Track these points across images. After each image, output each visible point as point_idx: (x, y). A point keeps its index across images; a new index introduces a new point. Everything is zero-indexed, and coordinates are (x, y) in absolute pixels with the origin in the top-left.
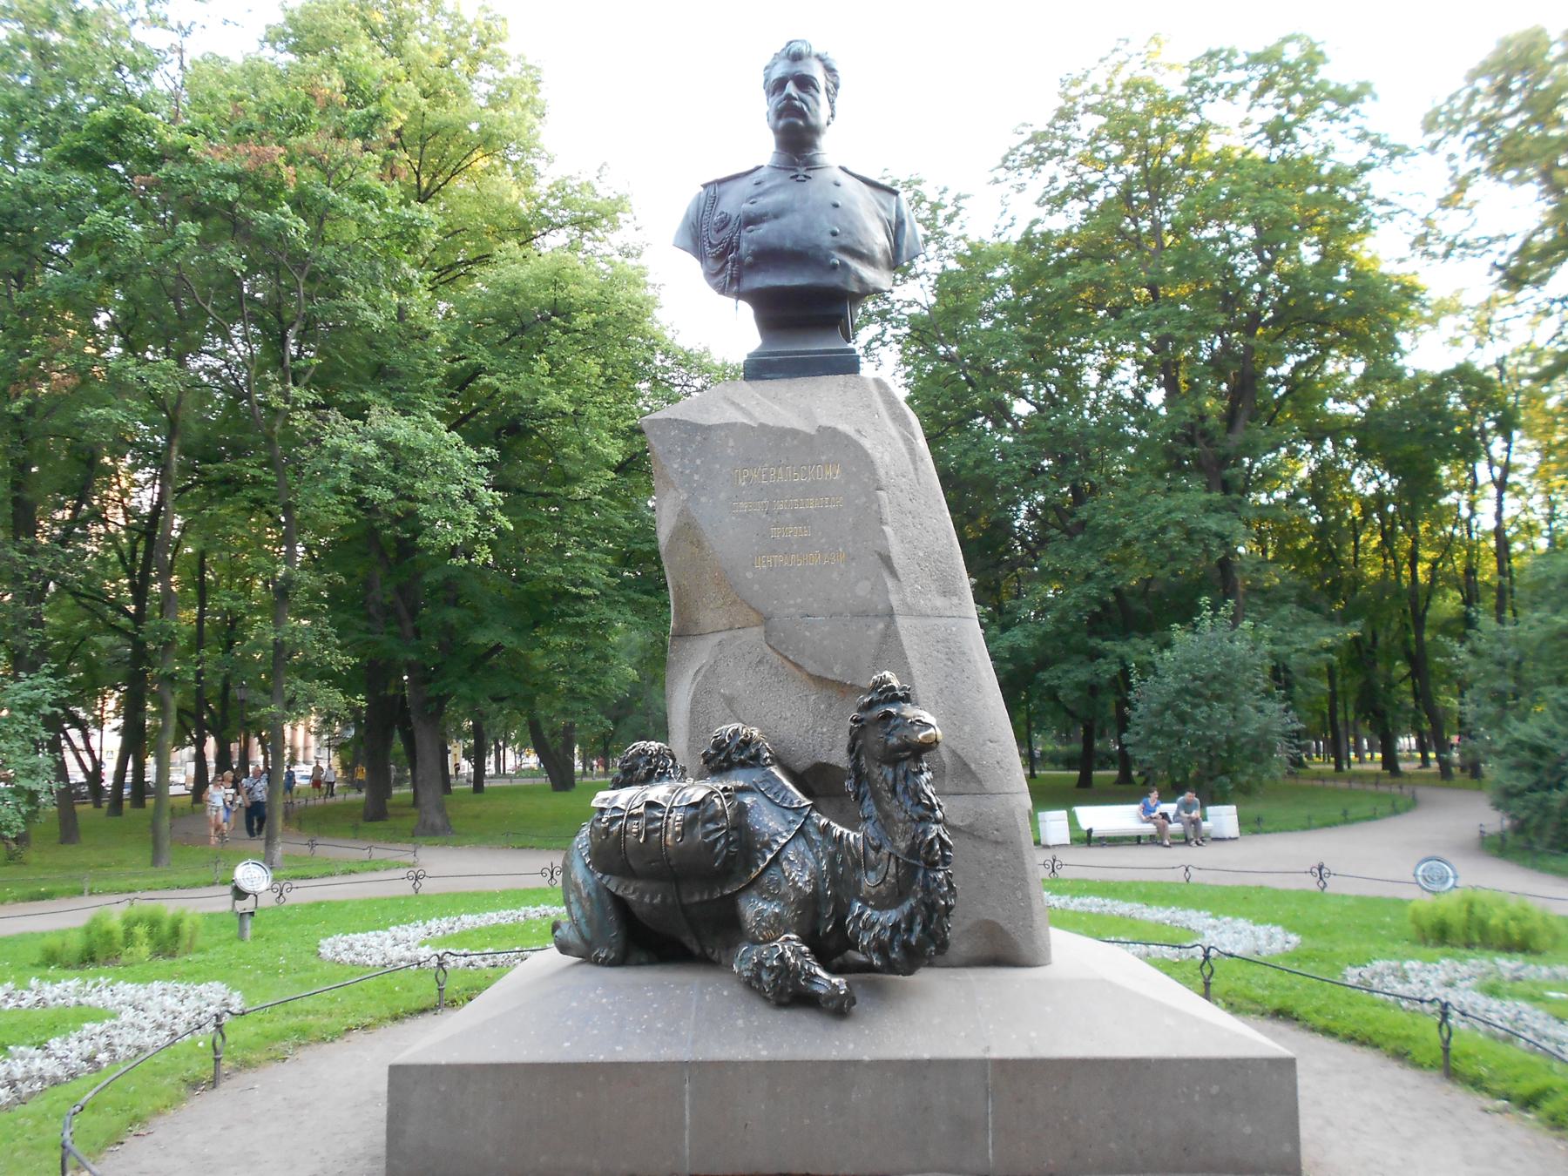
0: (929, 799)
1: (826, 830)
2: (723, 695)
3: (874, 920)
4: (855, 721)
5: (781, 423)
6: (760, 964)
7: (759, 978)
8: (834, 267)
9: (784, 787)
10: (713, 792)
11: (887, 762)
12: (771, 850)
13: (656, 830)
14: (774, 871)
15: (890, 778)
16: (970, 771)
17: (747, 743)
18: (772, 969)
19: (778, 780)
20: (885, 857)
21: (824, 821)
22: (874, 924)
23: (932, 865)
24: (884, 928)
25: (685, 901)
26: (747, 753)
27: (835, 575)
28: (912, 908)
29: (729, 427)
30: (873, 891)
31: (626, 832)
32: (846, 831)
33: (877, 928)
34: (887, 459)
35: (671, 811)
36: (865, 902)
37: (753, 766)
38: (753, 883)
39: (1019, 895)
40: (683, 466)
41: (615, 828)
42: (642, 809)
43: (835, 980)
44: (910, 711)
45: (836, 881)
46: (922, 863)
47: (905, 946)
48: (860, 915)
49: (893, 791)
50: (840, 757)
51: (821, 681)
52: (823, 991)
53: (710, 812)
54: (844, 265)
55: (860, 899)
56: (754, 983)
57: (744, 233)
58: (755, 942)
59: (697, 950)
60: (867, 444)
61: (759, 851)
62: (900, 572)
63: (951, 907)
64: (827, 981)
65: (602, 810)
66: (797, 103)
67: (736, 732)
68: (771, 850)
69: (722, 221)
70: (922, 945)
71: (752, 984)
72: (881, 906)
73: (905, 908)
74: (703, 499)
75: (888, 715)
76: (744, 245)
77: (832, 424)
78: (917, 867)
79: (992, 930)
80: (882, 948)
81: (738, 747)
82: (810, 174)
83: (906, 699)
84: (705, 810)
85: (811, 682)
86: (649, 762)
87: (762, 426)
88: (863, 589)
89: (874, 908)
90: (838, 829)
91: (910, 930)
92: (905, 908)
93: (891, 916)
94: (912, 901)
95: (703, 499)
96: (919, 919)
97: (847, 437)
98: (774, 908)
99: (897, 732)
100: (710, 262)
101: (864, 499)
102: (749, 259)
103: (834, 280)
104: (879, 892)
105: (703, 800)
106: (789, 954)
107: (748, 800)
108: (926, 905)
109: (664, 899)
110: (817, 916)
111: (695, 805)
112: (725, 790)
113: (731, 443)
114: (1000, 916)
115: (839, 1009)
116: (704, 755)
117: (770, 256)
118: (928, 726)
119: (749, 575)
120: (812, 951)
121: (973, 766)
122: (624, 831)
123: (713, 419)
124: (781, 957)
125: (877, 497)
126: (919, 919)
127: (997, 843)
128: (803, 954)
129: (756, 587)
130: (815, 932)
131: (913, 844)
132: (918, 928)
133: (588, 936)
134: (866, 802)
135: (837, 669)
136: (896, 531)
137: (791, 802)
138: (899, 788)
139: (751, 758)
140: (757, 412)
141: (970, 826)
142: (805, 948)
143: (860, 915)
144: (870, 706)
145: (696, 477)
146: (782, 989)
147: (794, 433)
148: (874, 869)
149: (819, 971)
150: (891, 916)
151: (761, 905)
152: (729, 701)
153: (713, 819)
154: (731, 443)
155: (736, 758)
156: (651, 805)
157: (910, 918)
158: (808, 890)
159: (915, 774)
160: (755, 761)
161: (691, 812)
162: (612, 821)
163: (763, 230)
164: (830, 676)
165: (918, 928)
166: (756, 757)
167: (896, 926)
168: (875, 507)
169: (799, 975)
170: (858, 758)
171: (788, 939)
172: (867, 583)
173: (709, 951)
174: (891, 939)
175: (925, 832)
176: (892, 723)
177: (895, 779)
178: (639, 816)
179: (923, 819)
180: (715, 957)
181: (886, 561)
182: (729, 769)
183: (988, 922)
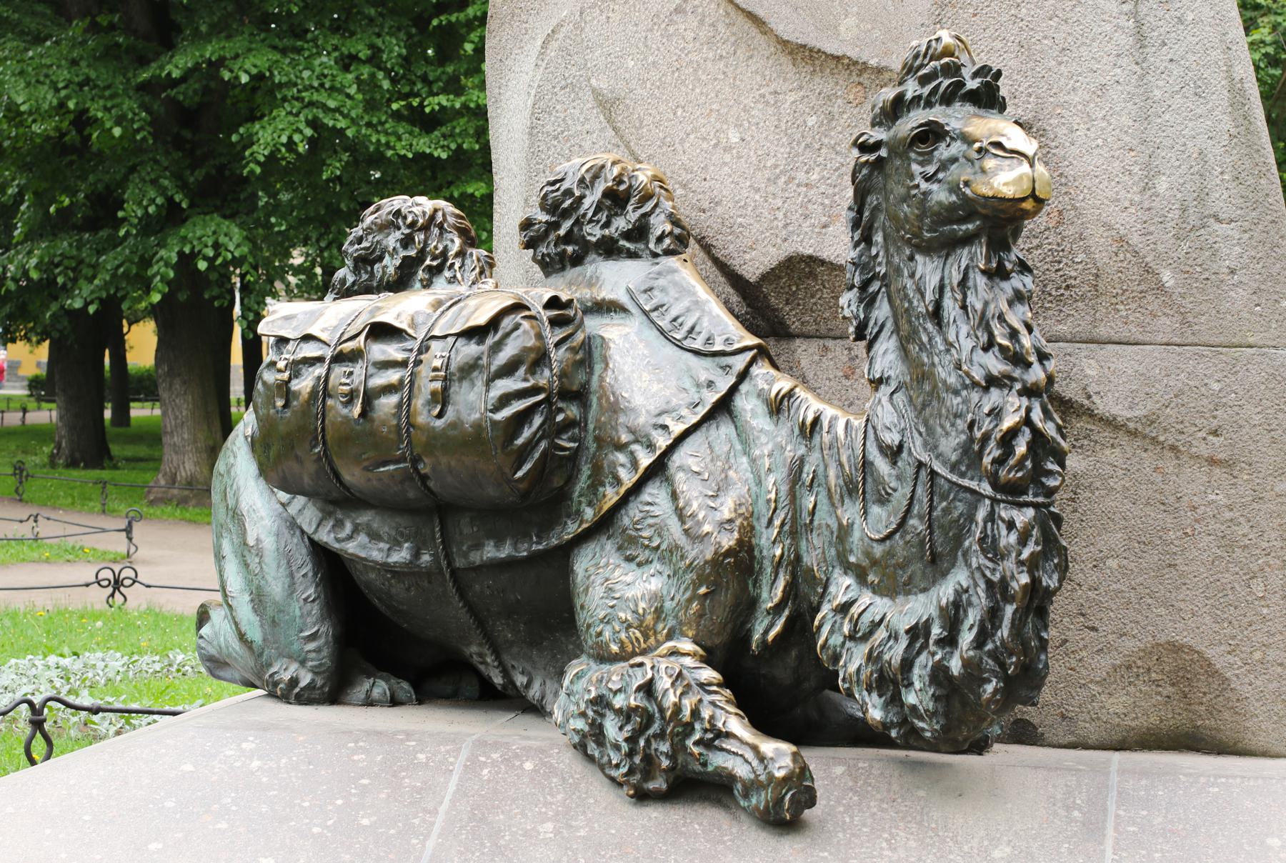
1: (778, 407)
2: (596, 93)
3: (868, 622)
4: (864, 148)
6: (601, 703)
7: (597, 733)
10: (518, 307)
11: (928, 249)
12: (650, 446)
13: (389, 389)
14: (655, 494)
15: (932, 282)
16: (1161, 287)
18: (626, 715)
19: (689, 292)
20: (910, 471)
21: (783, 384)
22: (875, 625)
24: (894, 636)
25: (459, 563)
26: (621, 224)
28: (960, 592)
30: (878, 550)
31: (327, 394)
32: (829, 412)
33: (881, 634)
35: (424, 348)
36: (861, 575)
37: (633, 255)
38: (605, 524)
41: (304, 384)
43: (769, 747)
44: (985, 126)
45: (796, 529)
46: (986, 488)
48: (844, 608)
49: (936, 314)
50: (838, 245)
51: (805, 56)
55: (848, 568)
56: (592, 748)
58: (604, 657)
59: (498, 680)
63: (1049, 594)
67: (598, 172)
68: (650, 446)
71: (589, 743)
72: (890, 589)
73: (945, 592)
78: (978, 496)
79: (1182, 669)
80: (889, 682)
81: (599, 208)
83: (988, 97)
85: (785, 59)
89: (877, 590)
91: (950, 641)
92: (945, 592)
93: (919, 607)
94: (959, 577)
96: (973, 616)
104: (890, 554)
105: (494, 323)
106: (664, 683)
109: (416, 554)
110: (748, 606)
112: (553, 303)
114: (1197, 630)
116: (527, 225)
121: (1167, 277)
122: (323, 390)
124: (648, 689)
126: (973, 616)
127: (1212, 462)
130: (740, 638)
131: (971, 439)
132: (967, 638)
133: (255, 634)
134: (880, 347)
137: (709, 340)
138: (951, 308)
139: (627, 235)
141: (1151, 421)
142: (708, 674)
144: (897, 107)
148: (883, 500)
149: (736, 725)
150: (919, 607)
152: (607, 105)
153: (508, 370)
155: (594, 233)
156: (381, 331)
157: (953, 616)
158: (728, 541)
161: (470, 350)
162: (296, 367)
164: (831, 47)
165: (967, 638)
166: (639, 232)
167: (918, 633)
169: (689, 728)
170: (867, 239)
171: (674, 653)
173: (520, 680)
174: (907, 664)
175: (996, 413)
176: (943, 151)
177: (941, 288)
178: (355, 356)
179: (992, 382)
180: (534, 693)
182: (577, 260)
183: (1176, 648)
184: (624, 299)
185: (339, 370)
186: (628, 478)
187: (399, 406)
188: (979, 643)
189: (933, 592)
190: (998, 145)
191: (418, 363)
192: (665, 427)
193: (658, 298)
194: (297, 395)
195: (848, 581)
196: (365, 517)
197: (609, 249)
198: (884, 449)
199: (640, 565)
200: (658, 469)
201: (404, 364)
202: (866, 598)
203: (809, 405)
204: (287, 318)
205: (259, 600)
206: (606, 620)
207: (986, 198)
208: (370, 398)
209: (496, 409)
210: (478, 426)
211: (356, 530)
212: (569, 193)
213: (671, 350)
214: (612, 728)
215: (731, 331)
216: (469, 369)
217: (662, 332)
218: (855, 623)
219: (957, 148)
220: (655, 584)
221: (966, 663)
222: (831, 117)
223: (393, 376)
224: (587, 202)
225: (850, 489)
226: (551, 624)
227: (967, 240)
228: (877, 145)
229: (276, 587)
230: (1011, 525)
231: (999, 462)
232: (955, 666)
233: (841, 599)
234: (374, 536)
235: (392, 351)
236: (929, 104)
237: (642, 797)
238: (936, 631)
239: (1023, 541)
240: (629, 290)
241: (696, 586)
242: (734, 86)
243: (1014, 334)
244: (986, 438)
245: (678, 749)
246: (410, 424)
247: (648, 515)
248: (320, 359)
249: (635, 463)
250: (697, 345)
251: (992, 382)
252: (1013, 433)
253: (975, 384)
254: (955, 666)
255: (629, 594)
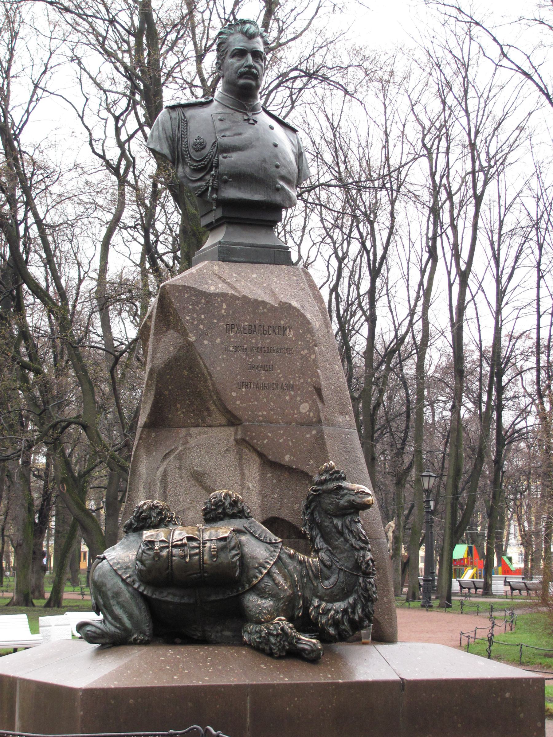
0: (365, 537)
4: (314, 491)
5: (256, 297)
6: (269, 634)
7: (268, 642)
8: (278, 190)
9: (264, 530)
13: (196, 554)
17: (235, 503)
18: (278, 635)
22: (329, 610)
23: (367, 574)
24: (337, 612)
27: (287, 398)
29: (224, 295)
31: (172, 556)
32: (306, 557)
33: (332, 612)
34: (318, 326)
35: (204, 543)
36: (321, 599)
39: (385, 599)
40: (193, 318)
41: (164, 553)
42: (185, 541)
46: (360, 574)
47: (352, 622)
48: (318, 606)
52: (306, 647)
53: (233, 544)
54: (283, 188)
55: (317, 597)
57: (221, 157)
58: (259, 622)
60: (308, 316)
61: (257, 568)
62: (325, 398)
64: (307, 641)
65: (152, 542)
66: (254, 71)
68: (265, 568)
69: (201, 144)
70: (361, 620)
73: (351, 600)
74: (206, 342)
75: (340, 488)
76: (221, 168)
77: (288, 301)
80: (336, 623)
81: (230, 504)
82: (255, 117)
83: (344, 479)
84: (230, 542)
86: (160, 513)
87: (244, 297)
88: (305, 408)
89: (327, 602)
90: (301, 557)
91: (353, 612)
92: (351, 600)
93: (340, 605)
95: (206, 342)
97: (298, 311)
98: (268, 603)
99: (347, 498)
100: (188, 170)
101: (306, 351)
102: (225, 177)
103: (278, 198)
104: (332, 592)
107: (243, 538)
108: (364, 597)
110: (294, 608)
111: (224, 539)
113: (224, 306)
115: (312, 659)
117: (240, 177)
118: (369, 494)
119: (234, 394)
120: (295, 627)
122: (170, 555)
123: (212, 289)
124: (282, 629)
125: (314, 350)
128: (290, 628)
129: (238, 402)
135: (287, 458)
136: (322, 372)
137: (270, 540)
139: (239, 512)
140: (238, 286)
142: (291, 625)
143: (318, 606)
145: (201, 327)
146: (284, 646)
147: (264, 303)
148: (327, 578)
151: (260, 601)
153: (233, 548)
154: (224, 306)
155: (230, 512)
156: (190, 539)
157: (353, 607)
159: (356, 522)
160: (241, 514)
161: (223, 543)
162: (162, 549)
163: (234, 157)
167: (345, 611)
168: (313, 357)
170: (312, 514)
171: (280, 620)
172: (307, 404)
175: (364, 557)
181: (318, 391)
184: (244, 529)
185: (175, 551)
186: (260, 576)
187: (200, 557)
188: (362, 612)
189: (347, 601)
190: (363, 492)
191: (204, 547)
192: (268, 563)
193: (253, 529)
194: (162, 556)
195: (317, 600)
196: (171, 591)
197: (233, 516)
198: (325, 565)
199: (265, 598)
200: (269, 574)
201: (198, 548)
202: (324, 604)
203: (301, 557)
204: (152, 535)
205: (131, 617)
206: (259, 613)
207: (361, 504)
208: (191, 556)
209: (233, 558)
210: (228, 563)
211: (169, 594)
212: (221, 501)
213: (261, 544)
214: (272, 640)
215: (274, 538)
216: (222, 549)
217: (256, 538)
218: (323, 610)
219: (345, 491)
220: (271, 603)
221: (359, 617)
222: (280, 481)
223: (197, 551)
224: (227, 503)
225: (316, 577)
226: (239, 615)
227: (350, 514)
228: (319, 490)
229: (136, 611)
230: (370, 583)
231: (366, 568)
232: (357, 617)
233: (316, 604)
234: (175, 595)
235: (195, 544)
236: (333, 480)
237: (280, 657)
238: (350, 610)
239: (373, 586)
240: (244, 527)
241: (284, 602)
242: (249, 472)
243: (365, 537)
244: (362, 562)
245: (290, 644)
246: (203, 563)
247: (267, 585)
248: (168, 547)
249: (261, 573)
250: (268, 541)
251: (362, 548)
252: (368, 561)
253: (356, 549)
254: (357, 617)
255: (266, 605)
